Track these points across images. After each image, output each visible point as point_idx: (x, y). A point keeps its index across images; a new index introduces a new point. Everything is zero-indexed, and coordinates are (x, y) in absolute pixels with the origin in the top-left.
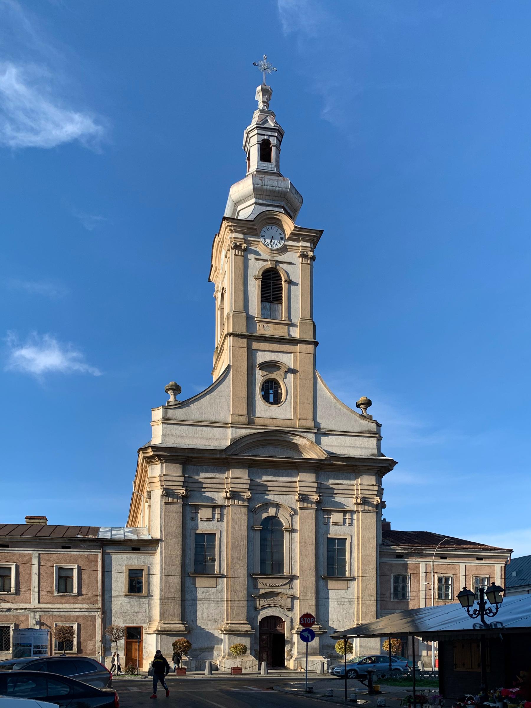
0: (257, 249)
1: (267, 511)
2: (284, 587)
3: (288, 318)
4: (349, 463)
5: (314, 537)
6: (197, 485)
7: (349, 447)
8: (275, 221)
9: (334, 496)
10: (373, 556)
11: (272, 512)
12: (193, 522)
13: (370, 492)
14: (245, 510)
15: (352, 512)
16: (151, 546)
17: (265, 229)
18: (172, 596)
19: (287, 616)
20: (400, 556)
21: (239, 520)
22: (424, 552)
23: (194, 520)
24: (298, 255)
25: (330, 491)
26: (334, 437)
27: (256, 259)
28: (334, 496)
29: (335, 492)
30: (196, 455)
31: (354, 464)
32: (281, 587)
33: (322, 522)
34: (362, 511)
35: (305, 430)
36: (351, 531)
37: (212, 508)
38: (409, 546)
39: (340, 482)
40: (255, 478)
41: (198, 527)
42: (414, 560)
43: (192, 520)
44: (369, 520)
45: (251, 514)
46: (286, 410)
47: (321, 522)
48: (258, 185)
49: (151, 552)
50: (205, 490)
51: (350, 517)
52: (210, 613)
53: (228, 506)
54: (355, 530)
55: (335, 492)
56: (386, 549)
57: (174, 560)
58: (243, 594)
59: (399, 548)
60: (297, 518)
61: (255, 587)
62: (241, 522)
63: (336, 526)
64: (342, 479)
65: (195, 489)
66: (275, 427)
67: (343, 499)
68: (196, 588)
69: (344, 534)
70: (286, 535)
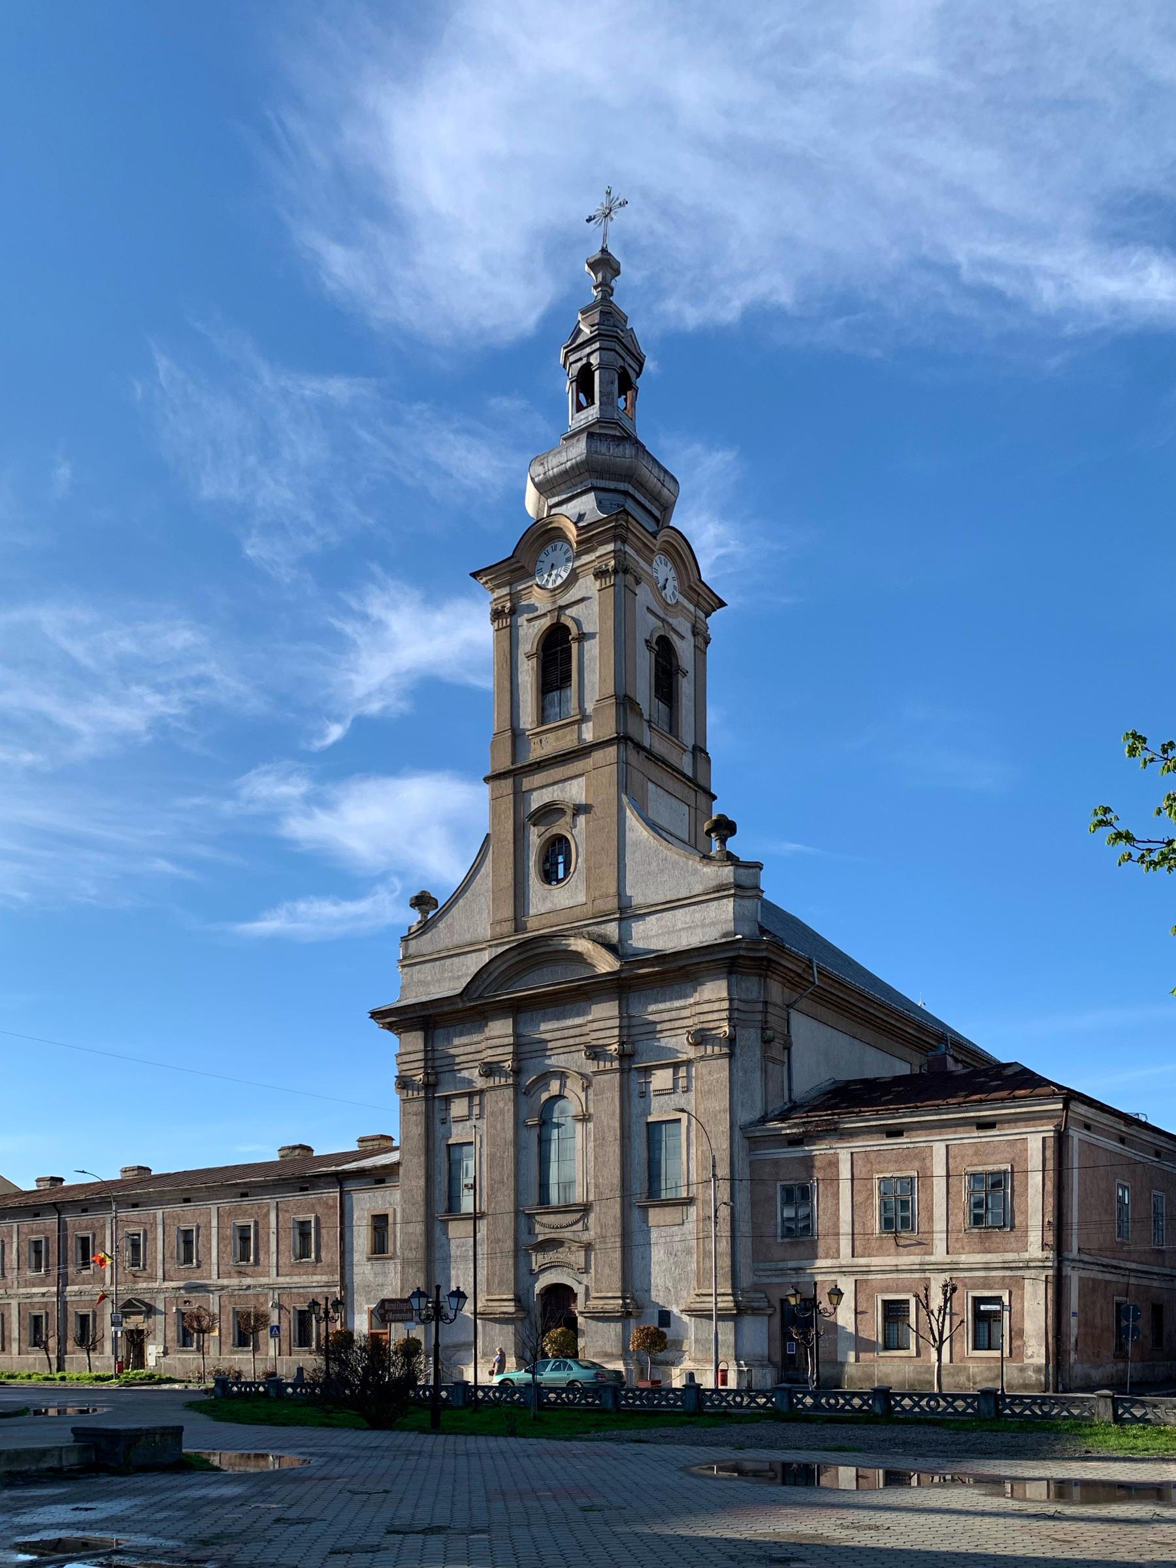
0: (533, 601)
1: (546, 1087)
2: (575, 1228)
3: (578, 710)
4: (666, 967)
5: (617, 1125)
6: (446, 1061)
7: (680, 930)
8: (553, 533)
9: (658, 1036)
10: (724, 1150)
11: (555, 1087)
13: (715, 1016)
14: (509, 1093)
15: (688, 1063)
17: (542, 557)
18: (413, 1257)
19: (580, 1283)
21: (502, 1112)
23: (445, 1123)
25: (649, 1028)
26: (653, 918)
27: (529, 620)
28: (658, 1036)
29: (659, 1027)
30: (431, 1012)
31: (674, 965)
32: (570, 1229)
33: (637, 1092)
35: (602, 918)
36: (689, 1101)
37: (467, 1098)
39: (668, 1005)
40: (523, 1031)
42: (824, 1147)
43: (442, 1123)
46: (577, 887)
47: (635, 1094)
48: (539, 475)
49: (396, 1184)
50: (458, 1067)
51: (685, 1075)
52: (466, 1283)
55: (659, 1027)
56: (759, 1130)
57: (415, 1195)
58: (509, 1245)
59: (783, 1125)
61: (531, 1231)
62: (504, 1115)
63: (662, 1097)
64: (671, 999)
65: (446, 1069)
66: (552, 927)
67: (674, 1039)
68: (448, 1240)
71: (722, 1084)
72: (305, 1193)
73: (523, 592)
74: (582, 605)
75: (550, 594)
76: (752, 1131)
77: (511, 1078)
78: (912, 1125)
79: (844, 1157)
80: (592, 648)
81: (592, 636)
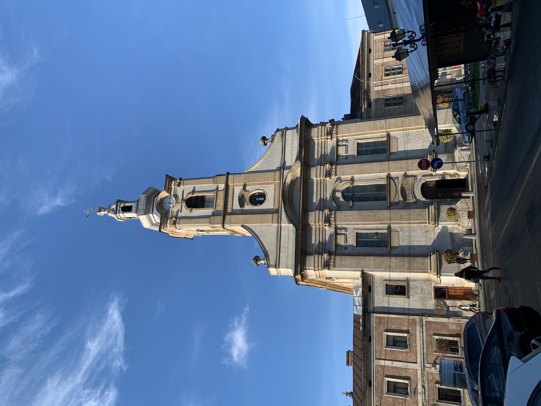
5: (357, 165)
9: (326, 154)
11: (339, 195)
12: (347, 248)
14: (338, 213)
15: (338, 141)
16: (367, 278)
20: (369, 105)
21: (345, 216)
22: (366, 89)
23: (346, 247)
24: (178, 188)
28: (326, 154)
34: (337, 134)
36: (352, 140)
38: (362, 100)
41: (352, 245)
42: (372, 95)
43: (347, 249)
44: (343, 129)
45: (341, 209)
47: (346, 161)
49: (372, 278)
53: (335, 225)
54: (351, 138)
56: (365, 115)
59: (363, 106)
60: (343, 177)
62: (347, 215)
63: (348, 150)
67: (328, 147)
69: (354, 145)
70: (355, 184)
71: (347, 127)
72: (372, 337)
73: (172, 214)
74: (184, 193)
75: (177, 204)
76: (365, 117)
77: (332, 212)
78: (368, 42)
79: (377, 89)
80: (199, 187)
81: (194, 188)
